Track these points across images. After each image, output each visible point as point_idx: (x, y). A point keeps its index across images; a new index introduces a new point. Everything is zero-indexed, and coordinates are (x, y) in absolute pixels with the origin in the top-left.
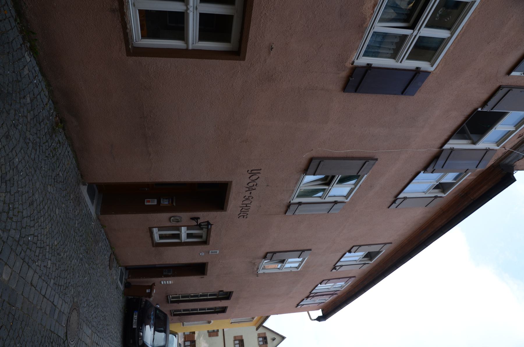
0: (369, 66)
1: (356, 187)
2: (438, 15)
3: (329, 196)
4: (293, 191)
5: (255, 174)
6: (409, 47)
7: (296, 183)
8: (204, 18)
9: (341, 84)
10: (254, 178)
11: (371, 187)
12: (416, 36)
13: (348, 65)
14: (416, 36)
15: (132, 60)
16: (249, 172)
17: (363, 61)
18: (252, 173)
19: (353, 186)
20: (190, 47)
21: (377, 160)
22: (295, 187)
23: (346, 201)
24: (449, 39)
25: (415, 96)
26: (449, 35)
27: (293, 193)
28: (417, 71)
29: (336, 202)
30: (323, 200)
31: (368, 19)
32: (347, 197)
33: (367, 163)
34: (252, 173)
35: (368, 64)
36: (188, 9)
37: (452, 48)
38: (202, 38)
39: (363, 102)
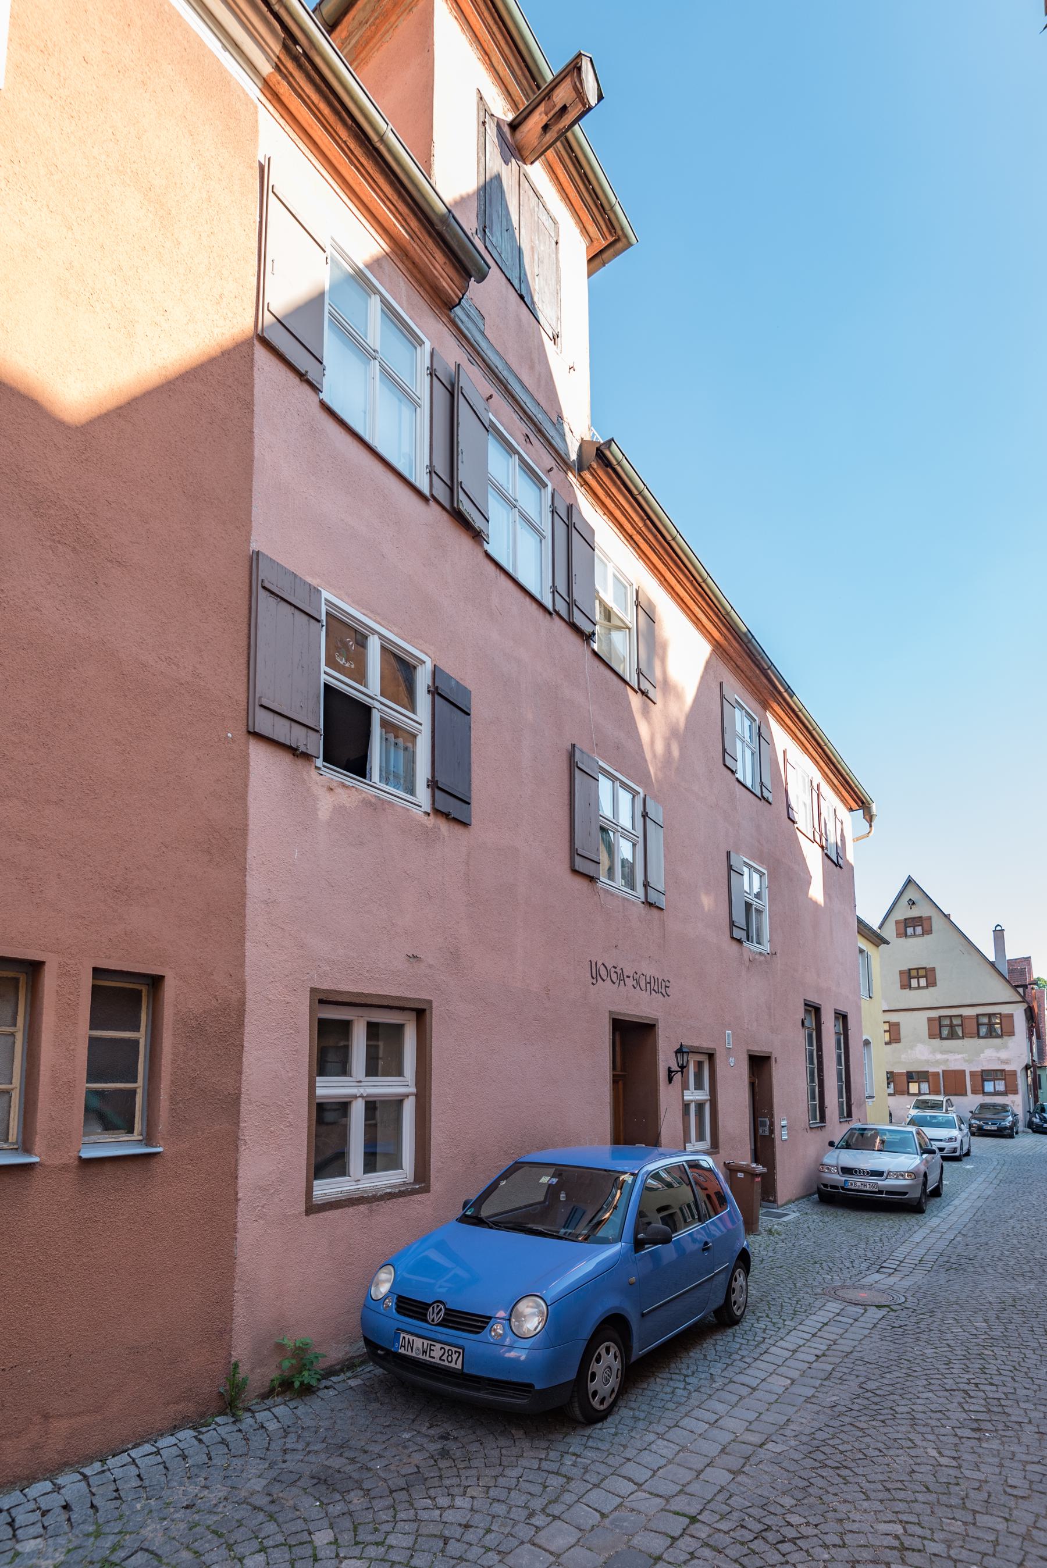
0: (433, 784)
1: (618, 779)
2: (347, 665)
3: (633, 828)
4: (624, 899)
5: (598, 971)
6: (398, 714)
7: (612, 895)
8: (372, 1070)
9: (458, 830)
10: (603, 972)
11: (618, 748)
12: (382, 703)
13: (431, 821)
14: (382, 703)
15: (436, 1185)
16: (594, 981)
17: (423, 795)
18: (596, 976)
19: (617, 783)
20: (413, 1090)
21: (573, 746)
22: (618, 897)
23: (642, 795)
24: (382, 637)
25: (469, 683)
26: (376, 637)
27: (628, 900)
28: (435, 692)
29: (645, 815)
30: (641, 840)
31: (364, 795)
32: (635, 794)
33: (580, 765)
34: (596, 976)
35: (428, 786)
36: (362, 1096)
37: (395, 629)
38: (399, 1073)
39: (484, 785)
